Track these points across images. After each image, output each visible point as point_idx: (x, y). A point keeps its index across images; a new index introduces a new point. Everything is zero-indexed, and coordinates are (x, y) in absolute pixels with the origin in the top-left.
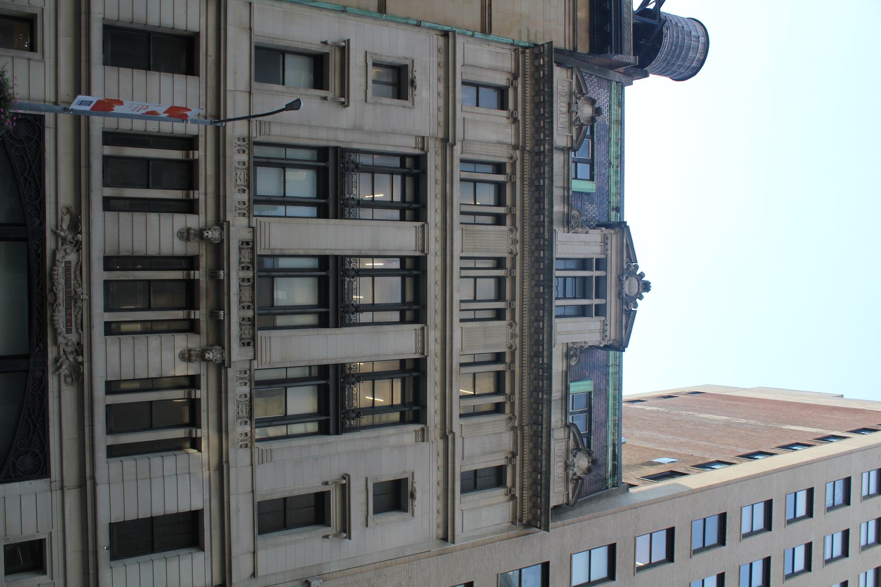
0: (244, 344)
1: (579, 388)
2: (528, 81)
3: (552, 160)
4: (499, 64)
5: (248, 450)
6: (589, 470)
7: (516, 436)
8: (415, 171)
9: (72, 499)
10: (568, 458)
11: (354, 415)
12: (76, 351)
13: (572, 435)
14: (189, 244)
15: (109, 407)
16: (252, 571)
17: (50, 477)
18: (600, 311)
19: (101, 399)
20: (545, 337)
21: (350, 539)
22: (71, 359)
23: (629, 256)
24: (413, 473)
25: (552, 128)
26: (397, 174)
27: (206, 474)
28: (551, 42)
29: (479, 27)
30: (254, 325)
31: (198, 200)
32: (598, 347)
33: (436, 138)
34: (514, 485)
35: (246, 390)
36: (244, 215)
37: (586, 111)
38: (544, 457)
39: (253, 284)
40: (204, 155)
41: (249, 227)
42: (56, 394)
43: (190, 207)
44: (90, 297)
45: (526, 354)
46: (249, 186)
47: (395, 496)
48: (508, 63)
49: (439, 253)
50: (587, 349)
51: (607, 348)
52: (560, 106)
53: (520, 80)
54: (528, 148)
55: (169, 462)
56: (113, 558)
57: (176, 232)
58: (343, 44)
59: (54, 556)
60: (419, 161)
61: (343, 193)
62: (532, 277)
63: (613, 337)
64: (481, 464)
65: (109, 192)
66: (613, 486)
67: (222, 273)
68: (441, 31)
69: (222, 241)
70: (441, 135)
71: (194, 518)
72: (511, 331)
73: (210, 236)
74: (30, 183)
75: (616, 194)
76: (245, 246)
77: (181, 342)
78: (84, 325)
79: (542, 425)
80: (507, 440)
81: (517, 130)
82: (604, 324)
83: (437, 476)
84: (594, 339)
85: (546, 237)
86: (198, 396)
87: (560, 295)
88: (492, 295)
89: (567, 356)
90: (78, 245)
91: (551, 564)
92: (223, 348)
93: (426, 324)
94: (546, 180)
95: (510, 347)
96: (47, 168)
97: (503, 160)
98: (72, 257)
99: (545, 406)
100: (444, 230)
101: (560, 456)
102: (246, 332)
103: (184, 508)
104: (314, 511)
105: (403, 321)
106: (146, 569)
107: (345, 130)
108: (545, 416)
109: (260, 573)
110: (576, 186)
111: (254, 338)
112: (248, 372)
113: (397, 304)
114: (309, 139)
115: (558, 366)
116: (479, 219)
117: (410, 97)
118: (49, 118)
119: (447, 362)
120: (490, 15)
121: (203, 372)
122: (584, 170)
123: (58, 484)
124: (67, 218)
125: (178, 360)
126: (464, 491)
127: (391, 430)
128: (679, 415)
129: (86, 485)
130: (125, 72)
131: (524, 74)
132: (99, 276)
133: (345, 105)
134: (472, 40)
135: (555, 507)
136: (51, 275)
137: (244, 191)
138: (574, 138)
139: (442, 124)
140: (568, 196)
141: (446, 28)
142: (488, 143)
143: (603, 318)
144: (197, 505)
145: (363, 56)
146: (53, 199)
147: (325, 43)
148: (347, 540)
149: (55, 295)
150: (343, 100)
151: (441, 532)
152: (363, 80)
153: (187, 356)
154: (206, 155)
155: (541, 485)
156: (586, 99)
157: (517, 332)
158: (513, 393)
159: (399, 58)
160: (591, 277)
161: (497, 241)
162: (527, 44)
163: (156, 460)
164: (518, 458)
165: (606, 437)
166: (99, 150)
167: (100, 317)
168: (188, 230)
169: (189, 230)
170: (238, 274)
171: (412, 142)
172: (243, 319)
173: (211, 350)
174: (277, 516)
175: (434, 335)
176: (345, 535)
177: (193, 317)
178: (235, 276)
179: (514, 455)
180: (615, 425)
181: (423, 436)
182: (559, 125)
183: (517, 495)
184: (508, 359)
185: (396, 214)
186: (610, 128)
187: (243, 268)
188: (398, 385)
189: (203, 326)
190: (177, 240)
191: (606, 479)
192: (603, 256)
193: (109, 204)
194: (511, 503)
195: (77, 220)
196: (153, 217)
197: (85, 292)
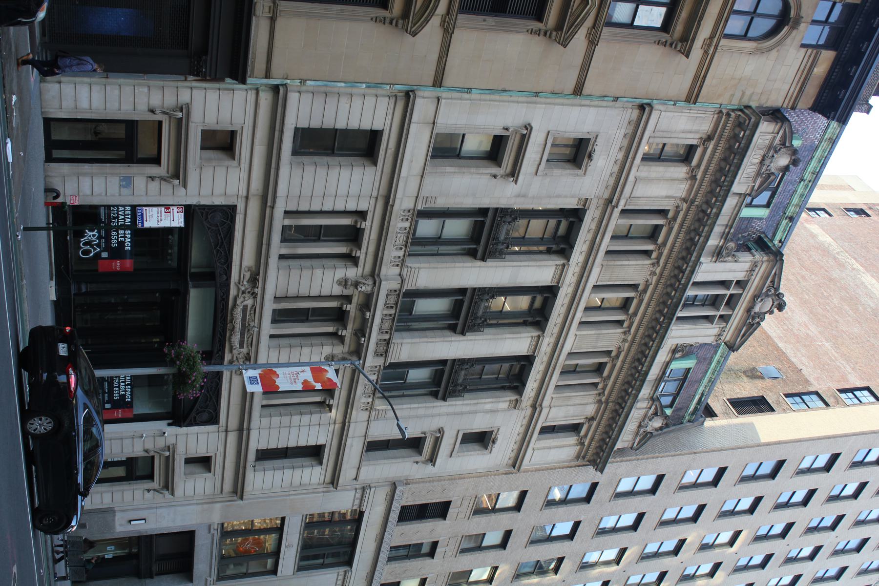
0: (377, 354)
1: (679, 365)
2: (722, 144)
3: (725, 200)
5: (367, 413)
9: (232, 437)
10: (643, 420)
19: (279, 221)
20: (651, 353)
21: (516, 183)
25: (735, 177)
27: (332, 427)
31: (359, 257)
35: (401, 253)
37: (783, 160)
39: (394, 318)
40: (370, 228)
41: (400, 275)
42: (228, 380)
43: (353, 260)
45: (631, 354)
53: (713, 143)
54: (696, 203)
56: (295, 153)
57: (336, 279)
59: (243, 146)
62: (658, 304)
66: (689, 421)
67: (368, 314)
71: (374, 137)
75: (797, 205)
79: (646, 357)
80: (680, 190)
81: (692, 187)
85: (682, 282)
90: (254, 295)
94: (702, 239)
96: (235, 243)
98: (249, 302)
100: (584, 268)
103: (366, 125)
106: (321, 172)
108: (628, 404)
117: (583, 167)
118: (240, 209)
119: (635, 144)
120: (701, 87)
123: (224, 429)
124: (248, 275)
128: (841, 266)
131: (720, 137)
136: (232, 314)
138: (756, 188)
140: (729, 232)
145: (544, 135)
146: (238, 263)
151: (511, 462)
152: (539, 156)
157: (630, 338)
158: (664, 244)
164: (595, 423)
166: (279, 221)
168: (346, 281)
170: (382, 311)
179: (709, 138)
180: (709, 381)
189: (347, 340)
191: (683, 417)
195: (256, 277)
197: (256, 325)
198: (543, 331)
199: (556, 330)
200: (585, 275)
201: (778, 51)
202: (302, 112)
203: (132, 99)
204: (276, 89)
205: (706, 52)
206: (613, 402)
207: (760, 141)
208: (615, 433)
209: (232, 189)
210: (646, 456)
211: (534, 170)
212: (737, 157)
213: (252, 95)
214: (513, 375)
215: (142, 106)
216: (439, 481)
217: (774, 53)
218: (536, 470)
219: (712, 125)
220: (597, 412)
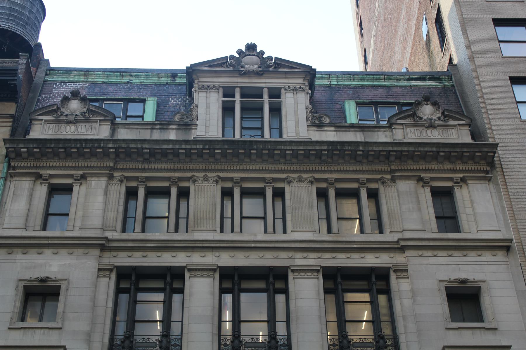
1: (352, 114)
4: (26, 193)
6: (435, 104)
8: (133, 279)
10: (422, 126)
11: (381, 341)
18: (275, 93)
23: (221, 65)
24: (440, 281)
25: (92, 140)
26: (136, 296)
28: (4, 140)
32: (312, 96)
33: (100, 257)
34: (451, 179)
37: (75, 105)
38: (422, 149)
45: (318, 167)
48: (26, 183)
49: (217, 254)
50: (313, 107)
51: (312, 86)
52: (69, 132)
53: (42, 172)
54: (112, 165)
63: (301, 81)
64: (430, 213)
66: (451, 80)
70: (97, 252)
72: (295, 183)
75: (159, 77)
79: (390, 151)
80: (405, 186)
83: (442, 257)
85: (201, 147)
87: (260, 133)
88: (260, 201)
89: (320, 126)
93: (287, 268)
94: (144, 146)
95: (312, 183)
97: (123, 189)
99: (370, 148)
100: (193, 249)
105: (285, 291)
108: (381, 148)
110: (150, 116)
113: (269, 297)
115: (330, 135)
116: (183, 214)
117: (58, 284)
122: (134, 109)
126: (457, 229)
127: (397, 304)
128: (379, 16)
131: (36, 167)
135: (473, 138)
138: (102, 118)
139: (86, 251)
140: (160, 124)
142: (106, 204)
143: (283, 91)
145: (13, 332)
151: (500, 253)
152: (38, 332)
155: (450, 152)
156: (63, 106)
157: (296, 176)
158: (357, 180)
159: (17, 295)
160: (242, 102)
161: (205, 196)
162: (6, 165)
164: (423, 175)
165: (401, 87)
171: (104, 282)
175: (300, 260)
179: (420, 179)
180: (389, 79)
181: (402, 271)
182: (89, 133)
183: (461, 175)
184: (324, 185)
185: (176, 298)
188: (350, 297)
191: (444, 87)
192: (221, 90)
194: (470, 182)
198: (388, 269)
199: (284, 255)
200: (200, 245)
206: (390, 166)
207: (413, 137)
208: (426, 149)
210: (482, 106)
211: (57, 332)
212: (48, 145)
218: (514, 219)
219: (24, 179)
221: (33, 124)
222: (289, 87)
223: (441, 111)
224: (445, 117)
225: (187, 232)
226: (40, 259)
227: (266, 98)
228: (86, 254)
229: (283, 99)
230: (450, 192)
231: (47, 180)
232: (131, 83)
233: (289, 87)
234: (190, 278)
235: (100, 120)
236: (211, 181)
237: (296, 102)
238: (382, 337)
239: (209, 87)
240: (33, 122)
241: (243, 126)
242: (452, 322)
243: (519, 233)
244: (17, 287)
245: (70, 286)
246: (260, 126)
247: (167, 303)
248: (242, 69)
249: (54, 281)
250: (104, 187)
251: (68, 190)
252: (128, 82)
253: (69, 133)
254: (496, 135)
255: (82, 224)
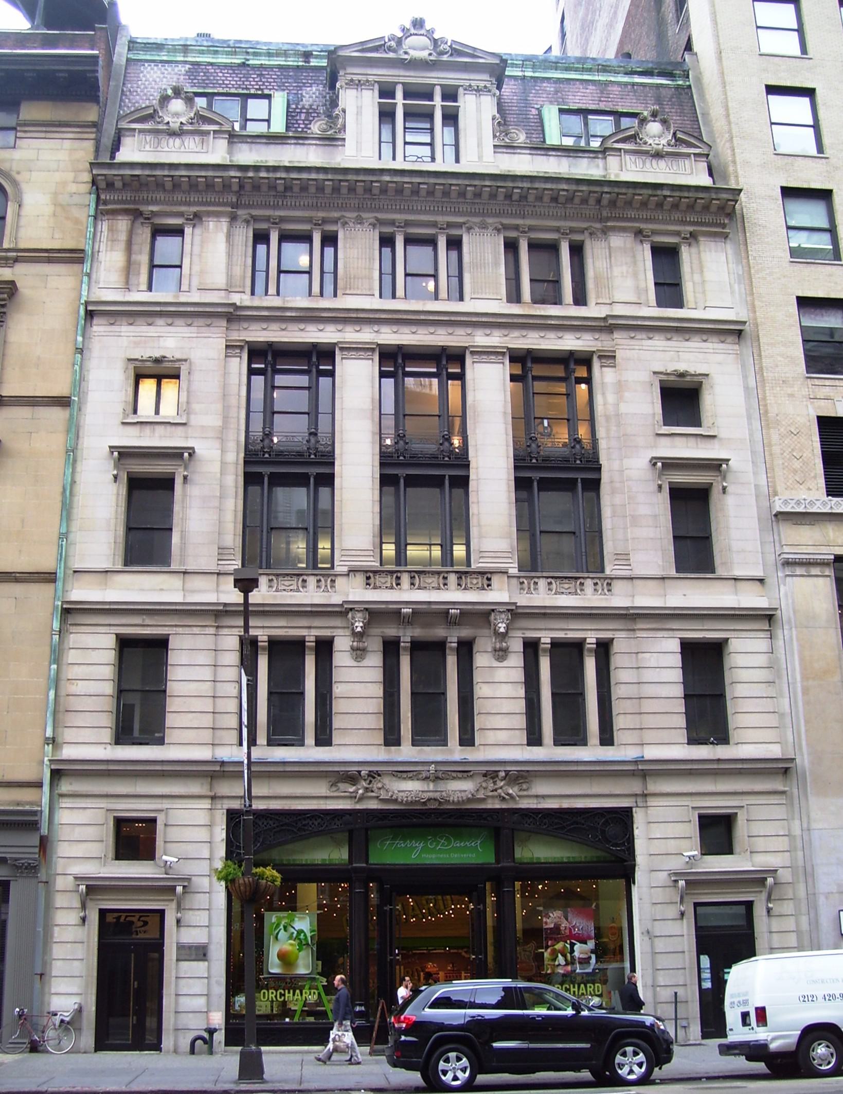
6: (664, 122)
7: (613, 229)
8: (270, 358)
11: (578, 446)
12: (492, 778)
13: (617, 146)
14: (370, 649)
15: (557, 742)
16: (758, 583)
17: (631, 808)
18: (450, 94)
22: (502, 784)
23: (376, 49)
29: (76, 267)
30: (466, 573)
32: (499, 99)
33: (227, 329)
34: (678, 234)
36: (333, 581)
43: (325, 648)
44: (432, 763)
46: (299, 575)
47: (681, 400)
49: (376, 328)
53: (143, 208)
55: (621, 675)
57: (355, 664)
58: (116, 454)
60: (256, 352)
61: (300, 454)
63: (486, 77)
65: (310, 739)
68: (85, 320)
69: (366, 609)
72: (477, 229)
73: (361, 624)
74: (304, 825)
76: (372, 581)
77: (482, 660)
78: (463, 771)
82: (469, 89)
83: (658, 342)
84: (488, 105)
86: (549, 641)
88: (429, 250)
89: (510, 148)
90: (372, 775)
91: (785, 185)
92: (493, 610)
95: (498, 230)
97: (251, 234)
101: (644, 163)
102: (475, 581)
104: (691, 504)
105: (461, 377)
107: (223, 451)
109: (759, 573)
110: (278, 126)
111: (482, 573)
112: (521, 580)
114: (236, 498)
115: (523, 164)
116: (329, 266)
121: (519, 634)
122: (256, 108)
123: (639, 800)
124: (342, 786)
125: (505, 664)
127: (599, 400)
129: (643, 771)
130: (171, 720)
131: (134, 202)
132: (407, 752)
133: (192, 452)
134: (94, 276)
136: (407, 803)
137: (304, 581)
138: (216, 127)
139: (209, 321)
141: (82, 312)
142: (230, 255)
143: (461, 91)
144: (675, 646)
146: (322, 802)
147: (116, 477)
148: (730, 462)
149: (429, 800)
150: (186, 455)
151: (730, 339)
153: (501, 653)
154: (263, 627)
156: (162, 108)
159: (127, 379)
160: (404, 104)
161: (358, 249)
162: (93, 196)
163: (618, 692)
165: (619, 84)
167: (454, 752)
169: (353, 649)
172: (459, 585)
173: (495, 625)
174: (694, 549)
175: (482, 339)
176: (724, 466)
177: (455, 645)
178: (407, 594)
181: (609, 357)
183: (691, 229)
185: (324, 382)
186: (194, 64)
187: (398, 584)
190: (366, 662)
191: (678, 87)
192: (377, 86)
193: (324, 738)
194: (701, 239)
195: (345, 775)
196: (338, 690)
197: (426, 768)
200: (354, 315)
201: (18, 173)
202: (90, 741)
203: (69, 945)
204: (56, 775)
205: (16, 260)
209: (202, 817)
213: (65, 803)
214: (550, 376)
215: (79, 933)
216: (770, 445)
217: (18, 178)
220: (624, 229)
221: (124, 136)
222: (470, 86)
223: (672, 131)
224: (676, 141)
225: (335, 295)
226: (151, 331)
227: (438, 101)
228: (209, 326)
229: (460, 103)
230: (675, 249)
231: (148, 219)
232: (248, 65)
233: (470, 86)
234: (342, 359)
235: (214, 131)
236: (366, 224)
237: (479, 110)
238: (578, 441)
239: (359, 81)
240: (123, 132)
241: (407, 140)
242: (664, 425)
243: (755, 312)
244: (127, 368)
245: (193, 368)
246: (429, 141)
247: (314, 389)
248: (406, 57)
249: (172, 361)
250: (225, 230)
251: (178, 232)
252: (244, 63)
253: (173, 149)
254: (740, 172)
255: (200, 283)
